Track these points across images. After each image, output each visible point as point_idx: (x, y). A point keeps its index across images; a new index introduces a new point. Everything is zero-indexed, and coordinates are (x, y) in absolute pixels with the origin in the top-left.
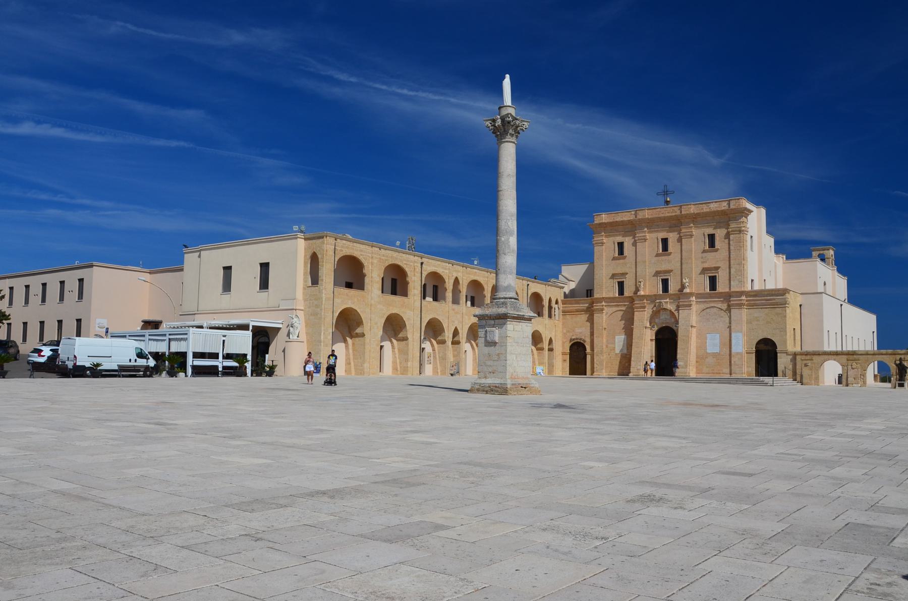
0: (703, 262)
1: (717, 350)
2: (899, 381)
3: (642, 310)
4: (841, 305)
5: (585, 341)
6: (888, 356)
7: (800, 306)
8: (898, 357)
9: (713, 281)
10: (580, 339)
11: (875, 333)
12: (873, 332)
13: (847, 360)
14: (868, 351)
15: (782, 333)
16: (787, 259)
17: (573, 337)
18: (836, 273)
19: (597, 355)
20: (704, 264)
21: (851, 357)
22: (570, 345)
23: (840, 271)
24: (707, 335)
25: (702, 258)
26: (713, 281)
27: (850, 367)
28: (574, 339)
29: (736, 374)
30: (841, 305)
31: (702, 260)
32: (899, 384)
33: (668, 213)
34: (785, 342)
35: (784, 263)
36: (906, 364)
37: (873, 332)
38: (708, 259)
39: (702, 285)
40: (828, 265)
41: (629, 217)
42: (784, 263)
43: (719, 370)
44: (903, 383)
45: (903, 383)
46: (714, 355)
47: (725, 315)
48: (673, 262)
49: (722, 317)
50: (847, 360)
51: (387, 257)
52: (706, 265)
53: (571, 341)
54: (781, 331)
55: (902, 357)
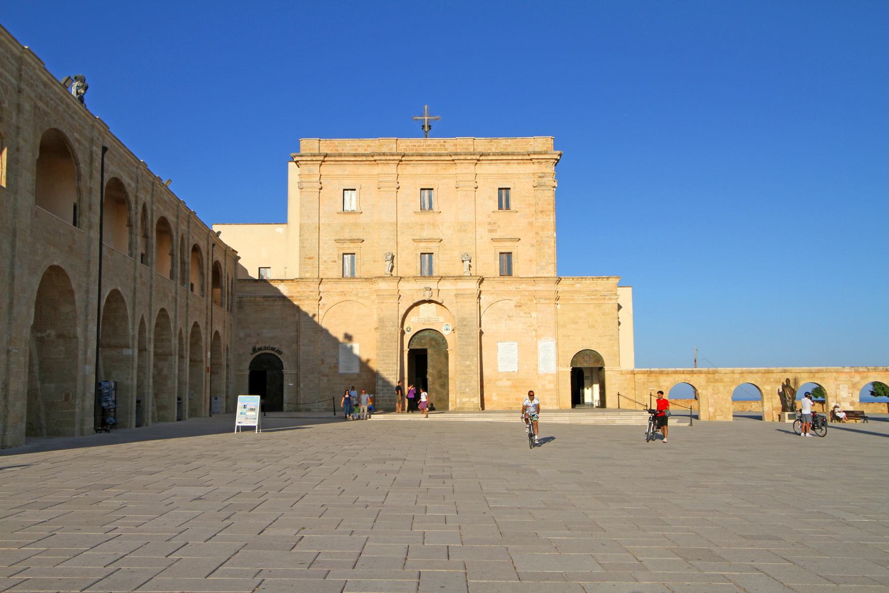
0: (491, 231)
1: (514, 368)
3: (392, 301)
5: (280, 353)
9: (506, 260)
10: (273, 349)
15: (612, 342)
17: (258, 346)
19: (306, 377)
20: (493, 234)
22: (252, 358)
24: (499, 344)
25: (489, 224)
26: (506, 260)
28: (260, 349)
29: (546, 404)
31: (490, 228)
32: (789, 415)
33: (433, 149)
34: (618, 355)
38: (499, 226)
39: (490, 266)
41: (365, 150)
43: (517, 399)
46: (509, 376)
47: (525, 313)
48: (441, 228)
49: (522, 317)
51: (47, 104)
52: (496, 235)
53: (254, 350)
54: (609, 340)
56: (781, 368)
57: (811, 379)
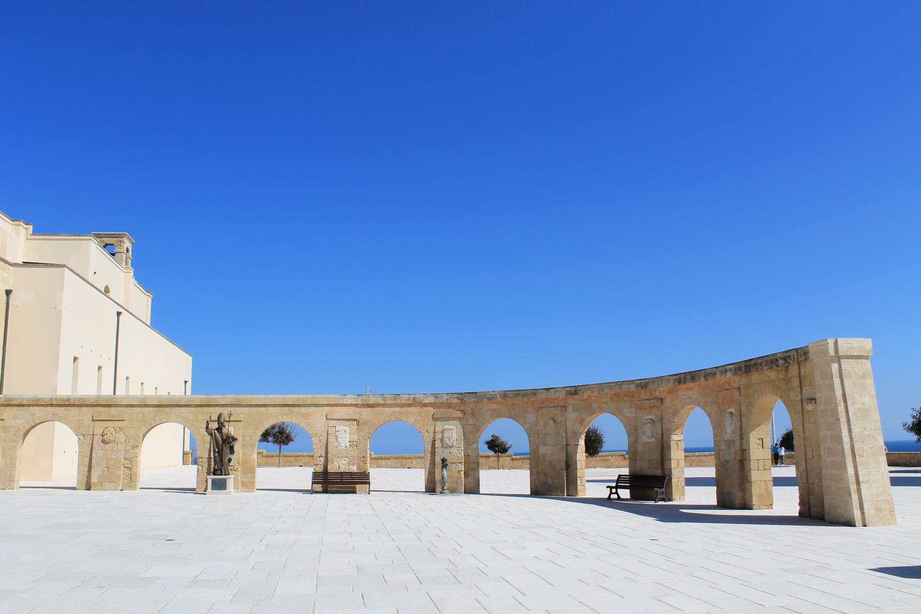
2: (214, 474)
4: (119, 314)
6: (193, 409)
7: (8, 292)
8: (214, 412)
11: (189, 385)
12: (186, 382)
13: (93, 420)
14: (145, 398)
16: (34, 233)
18: (133, 281)
21: (103, 412)
23: (143, 278)
27: (98, 439)
30: (119, 314)
35: (27, 239)
36: (231, 429)
37: (186, 382)
40: (120, 263)
42: (27, 239)
44: (225, 480)
45: (225, 480)
50: (93, 420)
55: (226, 411)
56: (232, 396)
57: (285, 416)
